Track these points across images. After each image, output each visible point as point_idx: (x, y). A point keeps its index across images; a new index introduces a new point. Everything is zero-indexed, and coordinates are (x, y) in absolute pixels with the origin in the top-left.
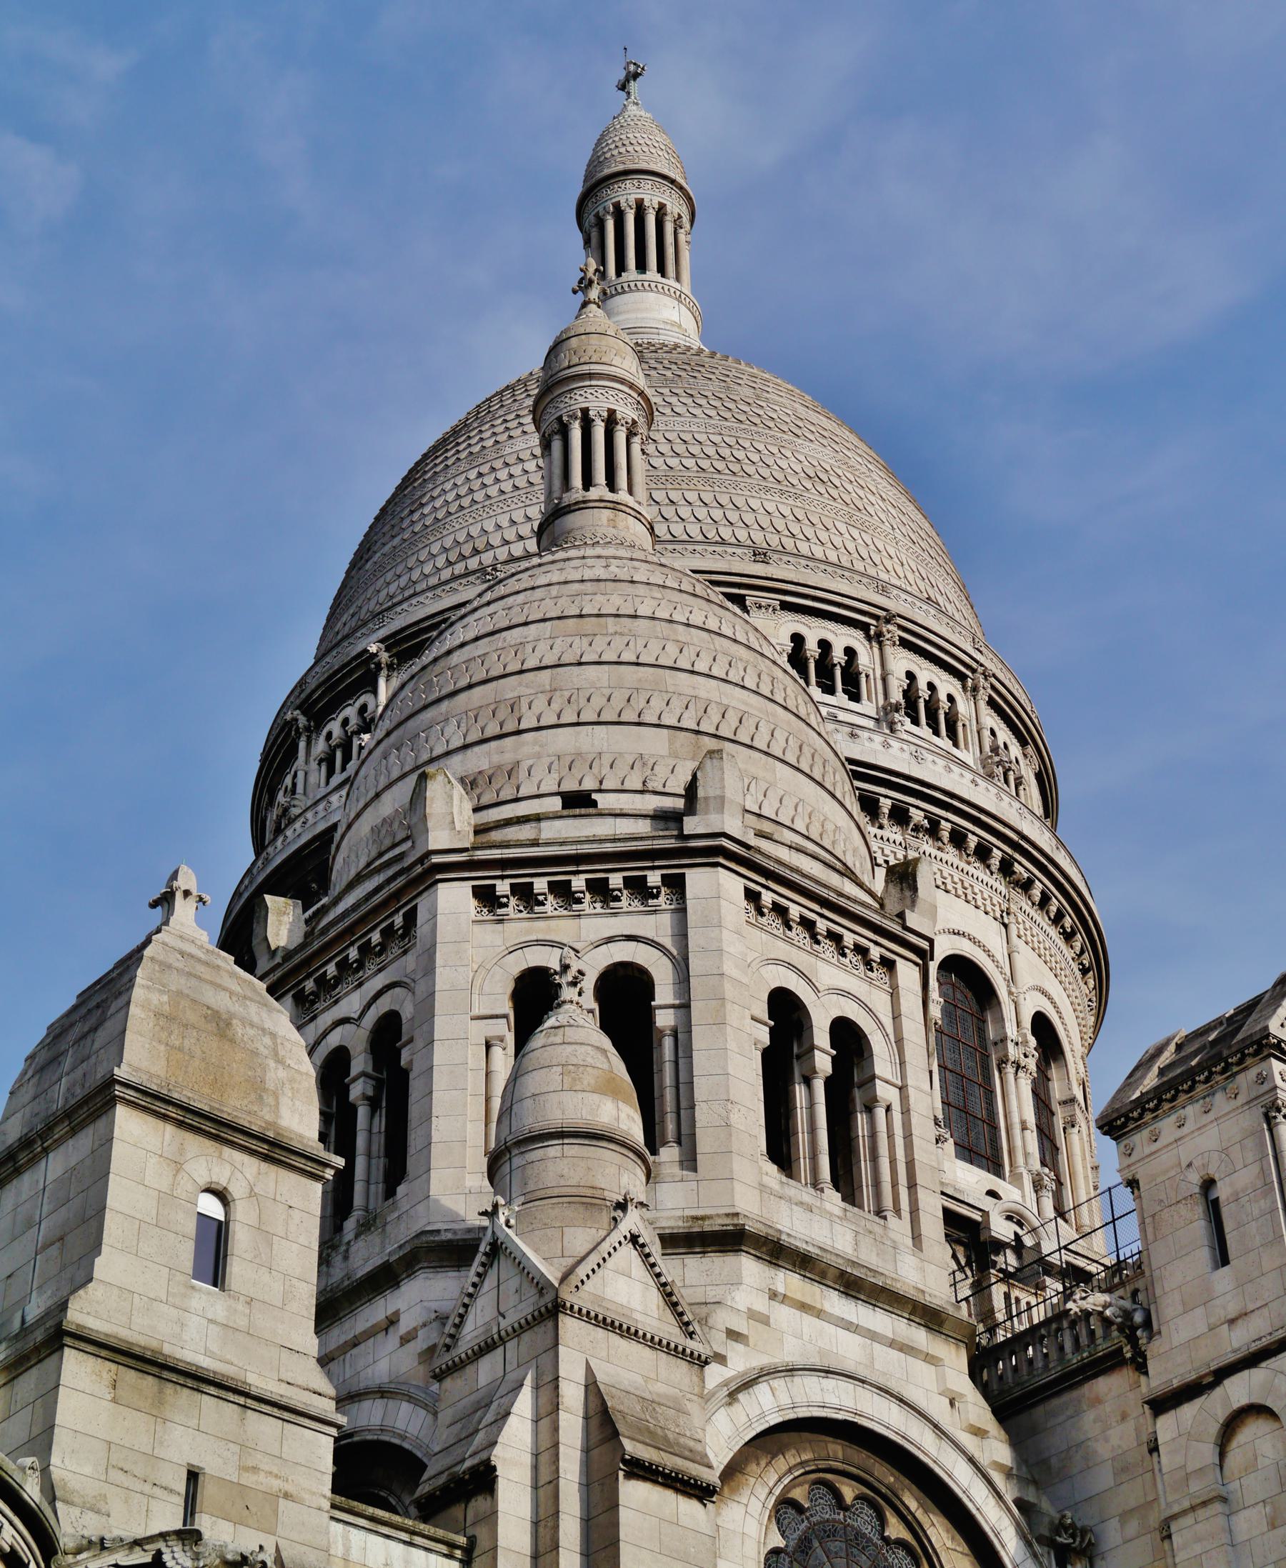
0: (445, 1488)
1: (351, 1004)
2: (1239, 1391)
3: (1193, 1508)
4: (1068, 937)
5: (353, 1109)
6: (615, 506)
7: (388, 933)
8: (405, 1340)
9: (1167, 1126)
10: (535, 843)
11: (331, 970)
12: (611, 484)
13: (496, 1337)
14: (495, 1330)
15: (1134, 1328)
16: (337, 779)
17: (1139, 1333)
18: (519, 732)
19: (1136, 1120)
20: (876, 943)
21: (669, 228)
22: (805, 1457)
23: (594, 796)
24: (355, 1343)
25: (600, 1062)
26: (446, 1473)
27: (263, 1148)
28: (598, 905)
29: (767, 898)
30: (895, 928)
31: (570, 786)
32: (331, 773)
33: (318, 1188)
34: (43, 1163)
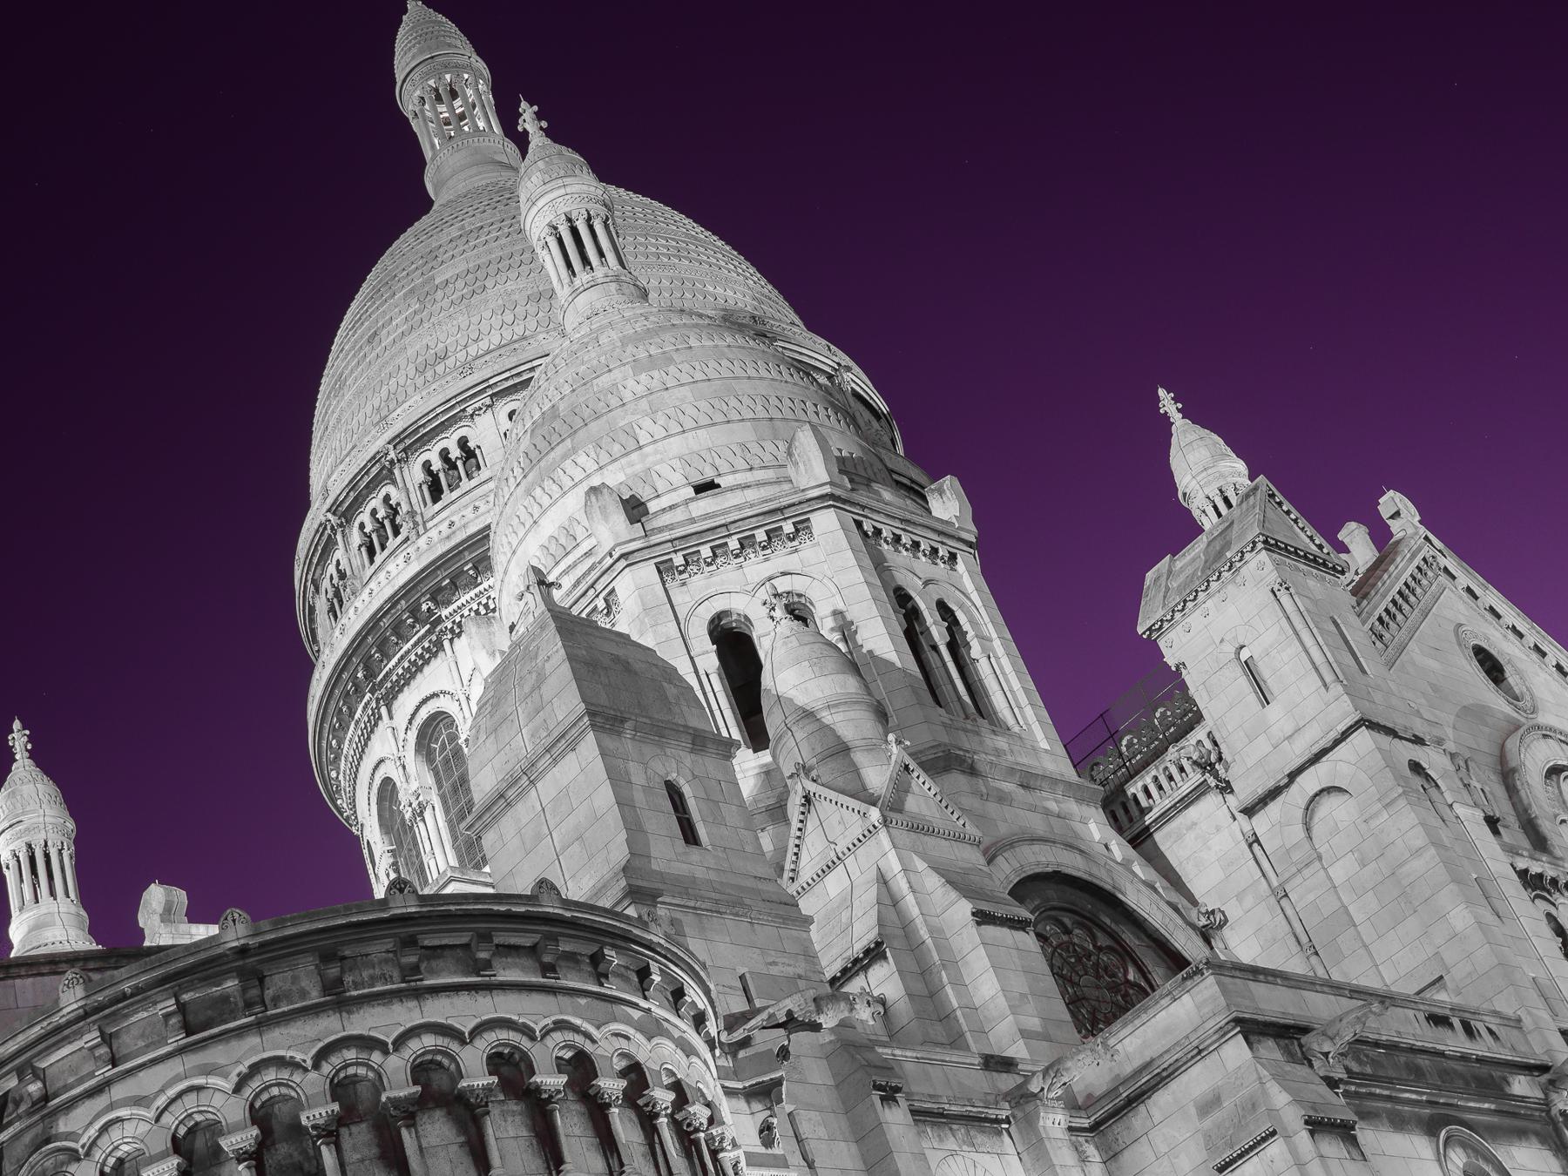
0: (845, 971)
2: (1310, 782)
3: (1299, 871)
9: (1195, 619)
10: (693, 521)
13: (835, 860)
14: (833, 854)
15: (1212, 765)
16: (379, 558)
17: (1217, 766)
18: (640, 448)
19: (1169, 621)
20: (943, 543)
22: (1036, 903)
23: (716, 481)
26: (839, 959)
28: (752, 556)
29: (867, 526)
31: (698, 479)
32: (371, 553)
34: (533, 792)
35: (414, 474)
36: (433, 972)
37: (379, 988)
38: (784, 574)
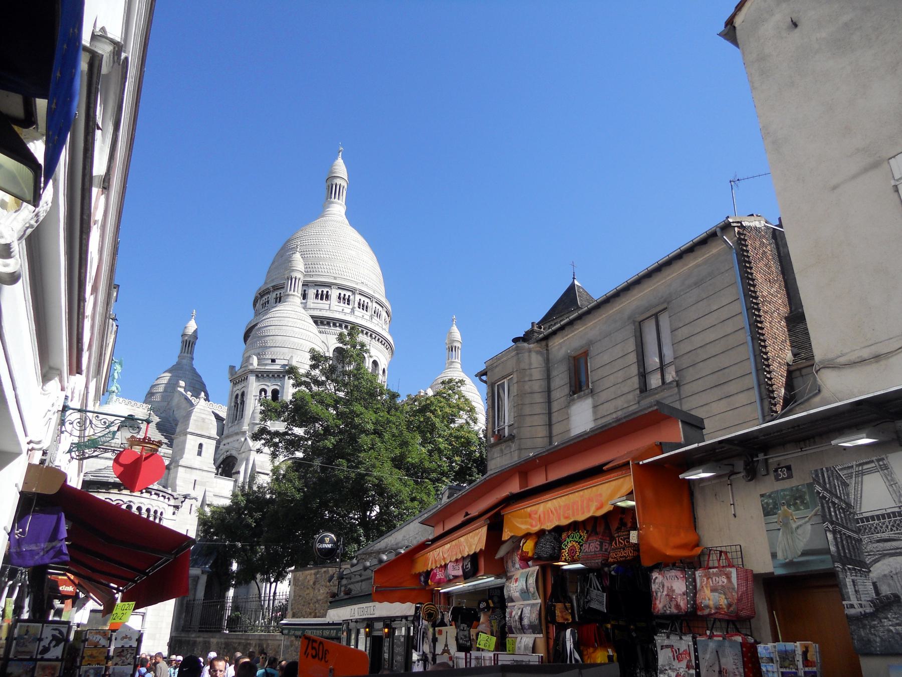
1: (240, 386)
4: (384, 345)
12: (294, 291)
16: (263, 310)
31: (272, 358)
35: (274, 295)
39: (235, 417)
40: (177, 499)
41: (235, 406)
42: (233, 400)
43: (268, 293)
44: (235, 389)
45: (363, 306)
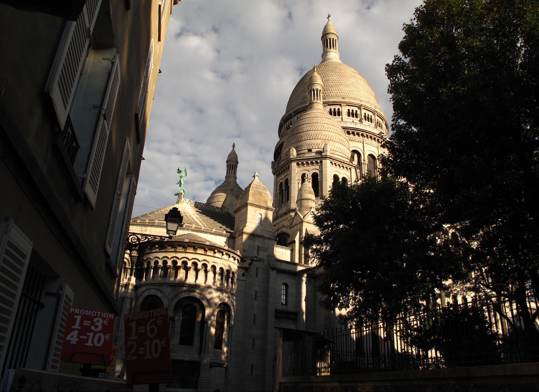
1: (283, 176)
5: (283, 190)
6: (318, 103)
7: (286, 168)
8: (289, 221)
11: (280, 172)
12: (317, 99)
21: (334, 41)
24: (283, 220)
25: (309, 190)
27: (266, 208)
29: (333, 163)
30: (351, 164)
31: (309, 148)
33: (272, 212)
36: (189, 250)
37: (181, 251)
38: (316, 169)
39: (281, 202)
40: (245, 261)
41: (280, 193)
42: (278, 188)
43: (291, 118)
44: (278, 180)
45: (368, 118)
